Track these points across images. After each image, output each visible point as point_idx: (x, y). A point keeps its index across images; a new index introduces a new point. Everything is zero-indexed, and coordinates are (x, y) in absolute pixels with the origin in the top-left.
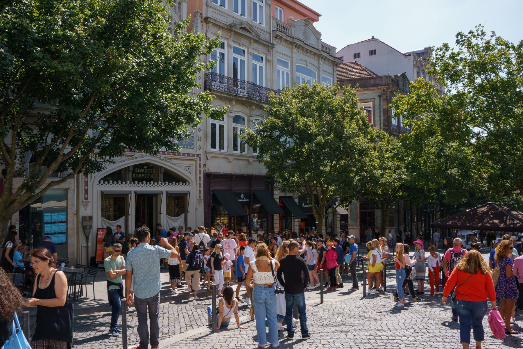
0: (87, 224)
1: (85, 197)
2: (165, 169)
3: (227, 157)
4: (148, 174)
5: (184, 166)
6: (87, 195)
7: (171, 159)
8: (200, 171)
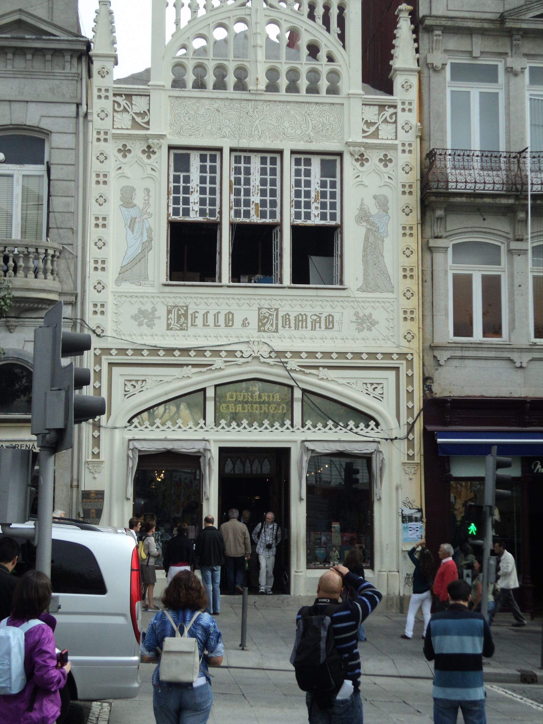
0: (90, 507)
1: (93, 453)
2: (304, 391)
3: (506, 355)
4: (260, 403)
5: (360, 383)
6: (99, 448)
7: (317, 367)
8: (410, 395)
